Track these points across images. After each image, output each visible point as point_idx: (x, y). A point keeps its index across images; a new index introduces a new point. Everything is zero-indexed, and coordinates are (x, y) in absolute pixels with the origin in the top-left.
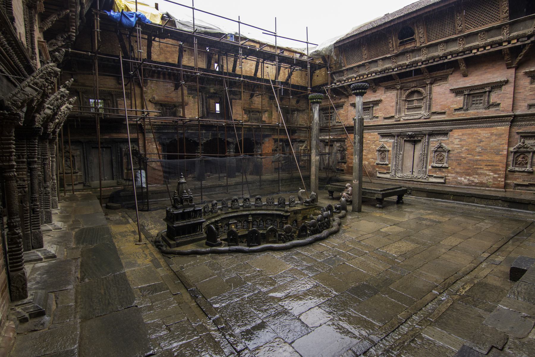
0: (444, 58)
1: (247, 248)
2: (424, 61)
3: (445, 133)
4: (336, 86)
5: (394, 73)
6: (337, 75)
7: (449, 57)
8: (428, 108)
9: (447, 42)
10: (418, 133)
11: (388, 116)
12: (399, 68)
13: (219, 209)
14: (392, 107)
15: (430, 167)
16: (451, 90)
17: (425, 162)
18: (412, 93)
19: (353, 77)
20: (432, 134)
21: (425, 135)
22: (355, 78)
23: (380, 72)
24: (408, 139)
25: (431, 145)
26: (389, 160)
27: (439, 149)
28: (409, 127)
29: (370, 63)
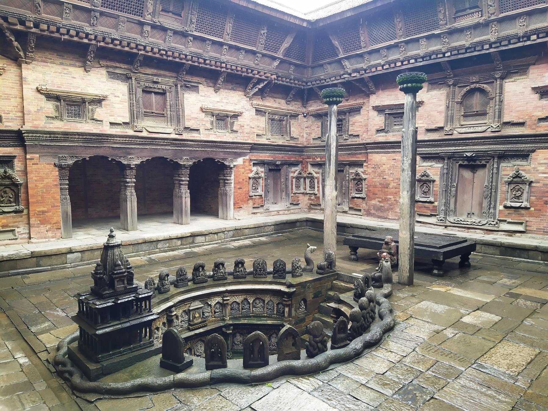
0: (525, 39)
1: (247, 373)
2: (495, 43)
3: (525, 156)
4: (351, 79)
5: (446, 59)
6: (353, 61)
7: (534, 37)
8: (497, 116)
9: (530, 14)
10: (481, 154)
11: (433, 127)
12: (453, 53)
13: (172, 283)
14: (440, 112)
15: (501, 208)
16: (534, 89)
17: (493, 198)
18: (471, 92)
19: (379, 64)
20: (503, 156)
21: (494, 158)
22: (383, 66)
23: (423, 58)
24: (466, 163)
25: (503, 173)
26: (435, 195)
27: (515, 180)
28: (467, 145)
29: (407, 42)
